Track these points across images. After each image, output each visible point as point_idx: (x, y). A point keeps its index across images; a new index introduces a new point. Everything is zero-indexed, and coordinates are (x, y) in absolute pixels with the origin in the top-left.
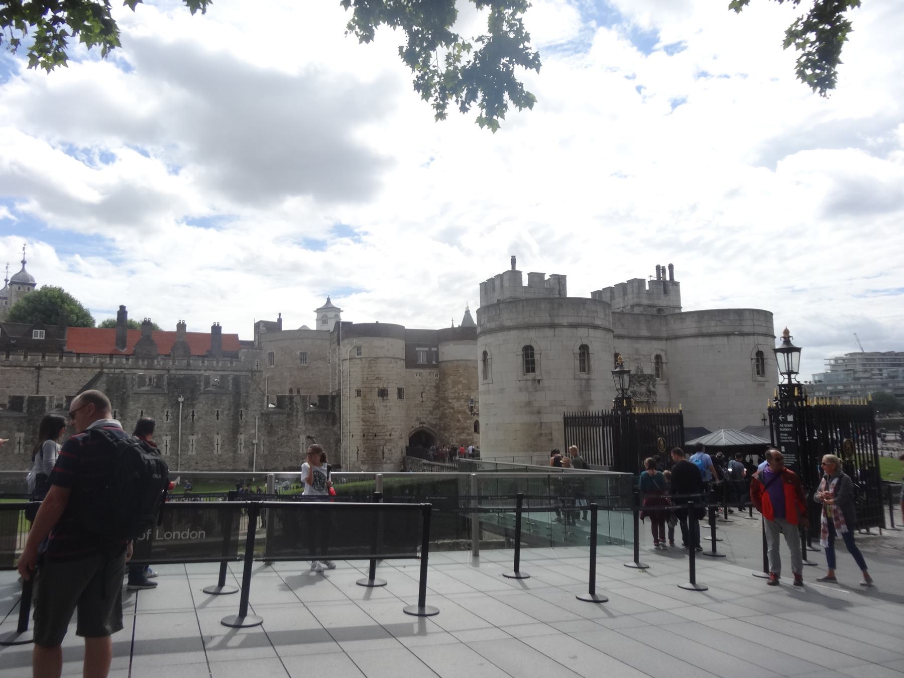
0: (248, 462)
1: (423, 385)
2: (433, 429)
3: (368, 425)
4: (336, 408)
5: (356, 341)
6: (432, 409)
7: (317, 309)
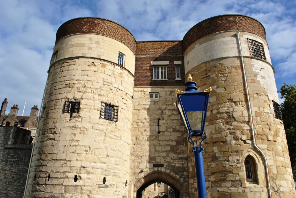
1: (160, 109)
2: (178, 177)
6: (174, 143)
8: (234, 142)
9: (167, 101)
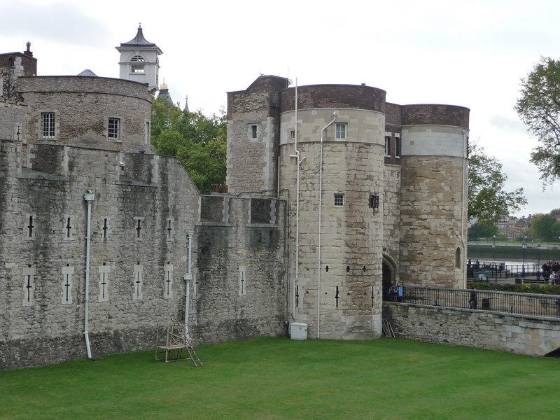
0: (176, 314)
3: (356, 253)
4: (280, 221)
5: (340, 114)
7: (122, 45)
8: (451, 237)
9: (389, 182)
